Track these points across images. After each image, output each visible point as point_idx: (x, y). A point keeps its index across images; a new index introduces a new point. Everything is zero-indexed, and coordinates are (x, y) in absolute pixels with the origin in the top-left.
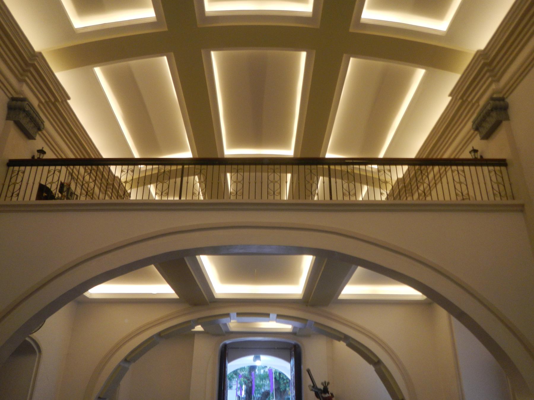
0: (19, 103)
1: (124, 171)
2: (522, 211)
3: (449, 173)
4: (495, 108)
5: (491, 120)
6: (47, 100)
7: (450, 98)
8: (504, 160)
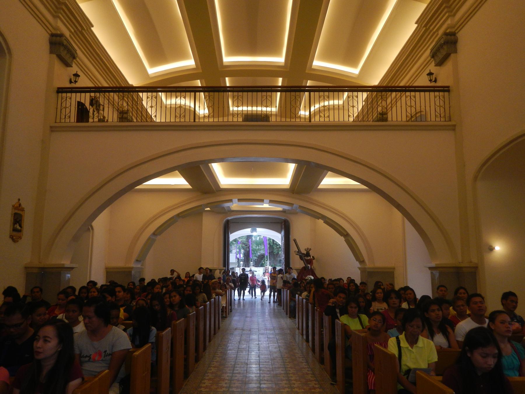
0: (58, 38)
1: (149, 98)
2: (454, 130)
3: (403, 98)
4: (446, 43)
5: (443, 52)
6: (76, 30)
7: (416, 25)
8: (448, 87)
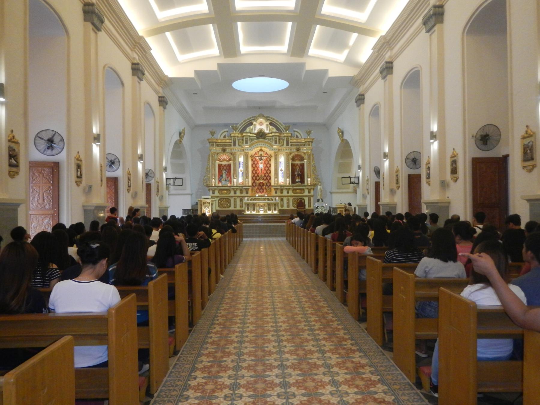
0: (90, 7)
5: (432, 21)
